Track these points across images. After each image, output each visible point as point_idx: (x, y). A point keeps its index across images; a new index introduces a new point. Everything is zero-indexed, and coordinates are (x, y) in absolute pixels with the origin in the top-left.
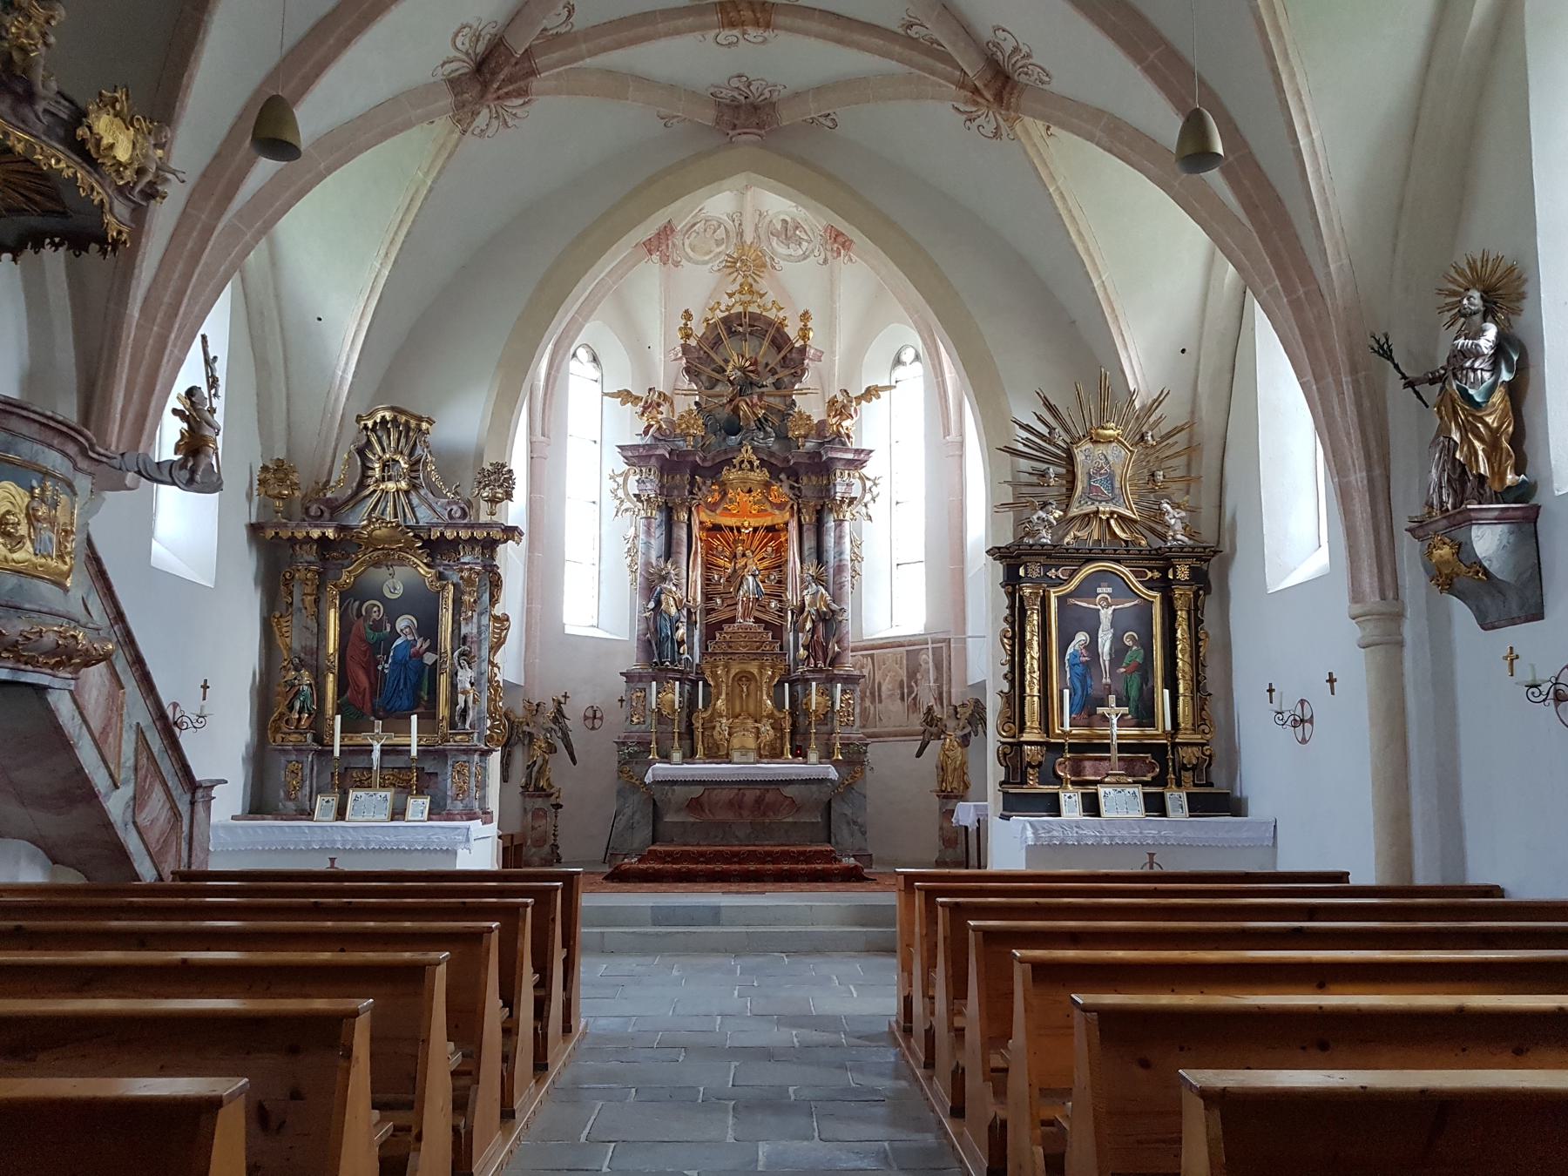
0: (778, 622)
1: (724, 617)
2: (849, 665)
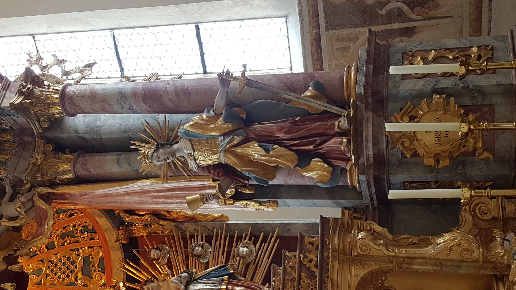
0: (273, 244)
2: (349, 71)
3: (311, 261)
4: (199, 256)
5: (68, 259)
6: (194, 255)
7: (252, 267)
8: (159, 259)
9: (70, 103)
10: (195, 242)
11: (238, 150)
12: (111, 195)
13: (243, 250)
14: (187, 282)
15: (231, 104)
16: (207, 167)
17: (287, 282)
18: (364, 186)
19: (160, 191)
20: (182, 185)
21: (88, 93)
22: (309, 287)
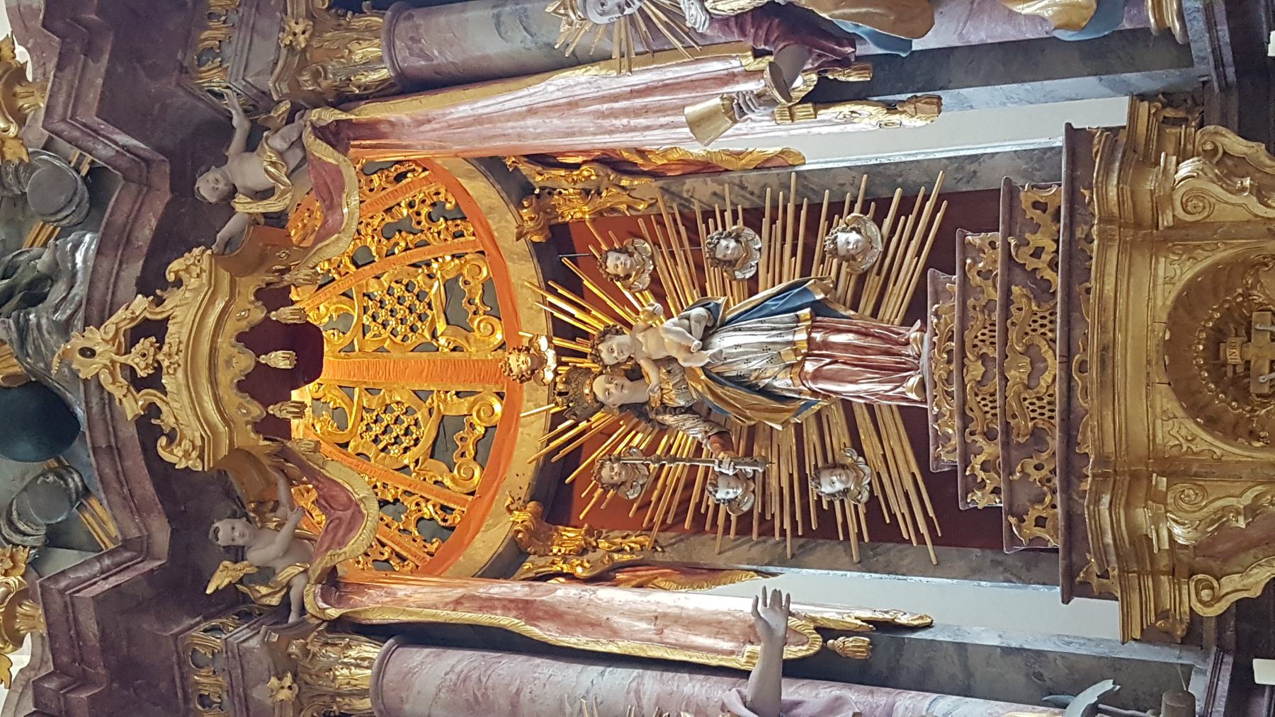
0: (930, 216)
1: (907, 464)
3: (1037, 253)
4: (731, 263)
6: (717, 262)
7: (873, 282)
8: (628, 276)
10: (716, 229)
13: (847, 239)
14: (707, 329)
16: (737, 16)
17: (971, 313)
19: (615, 98)
20: (670, 75)
22: (1035, 321)
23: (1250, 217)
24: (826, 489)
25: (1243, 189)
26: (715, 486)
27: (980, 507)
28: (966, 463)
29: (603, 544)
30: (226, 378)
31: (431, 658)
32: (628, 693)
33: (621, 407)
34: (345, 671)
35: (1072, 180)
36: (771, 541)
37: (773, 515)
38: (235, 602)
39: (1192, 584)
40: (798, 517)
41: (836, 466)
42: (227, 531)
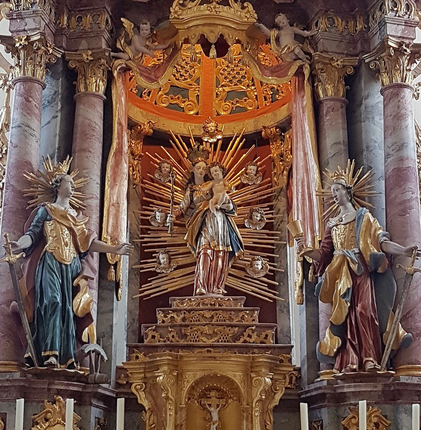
0: (267, 295)
1: (171, 287)
3: (249, 336)
4: (251, 218)
5: (243, 77)
6: (252, 211)
7: (242, 274)
8: (247, 174)
9: (394, 92)
10: (265, 211)
11: (345, 268)
12: (303, 137)
13: (259, 265)
14: (225, 210)
15: (391, 258)
16: (331, 236)
17: (229, 313)
18: (318, 385)
19: (308, 188)
20: (315, 209)
21: (403, 111)
22: (225, 335)
23: (253, 397)
24: (161, 256)
25: (261, 396)
26: (161, 212)
27: (157, 316)
28: (174, 311)
29: (136, 163)
30: (206, 30)
31: (100, 115)
32: (92, 194)
33: (193, 173)
34: (94, 81)
35: (274, 348)
36: (139, 233)
37: (149, 234)
38: (116, 29)
39: (141, 383)
40: (149, 244)
41: (170, 259)
42: (146, 28)
